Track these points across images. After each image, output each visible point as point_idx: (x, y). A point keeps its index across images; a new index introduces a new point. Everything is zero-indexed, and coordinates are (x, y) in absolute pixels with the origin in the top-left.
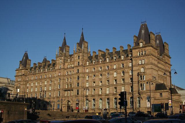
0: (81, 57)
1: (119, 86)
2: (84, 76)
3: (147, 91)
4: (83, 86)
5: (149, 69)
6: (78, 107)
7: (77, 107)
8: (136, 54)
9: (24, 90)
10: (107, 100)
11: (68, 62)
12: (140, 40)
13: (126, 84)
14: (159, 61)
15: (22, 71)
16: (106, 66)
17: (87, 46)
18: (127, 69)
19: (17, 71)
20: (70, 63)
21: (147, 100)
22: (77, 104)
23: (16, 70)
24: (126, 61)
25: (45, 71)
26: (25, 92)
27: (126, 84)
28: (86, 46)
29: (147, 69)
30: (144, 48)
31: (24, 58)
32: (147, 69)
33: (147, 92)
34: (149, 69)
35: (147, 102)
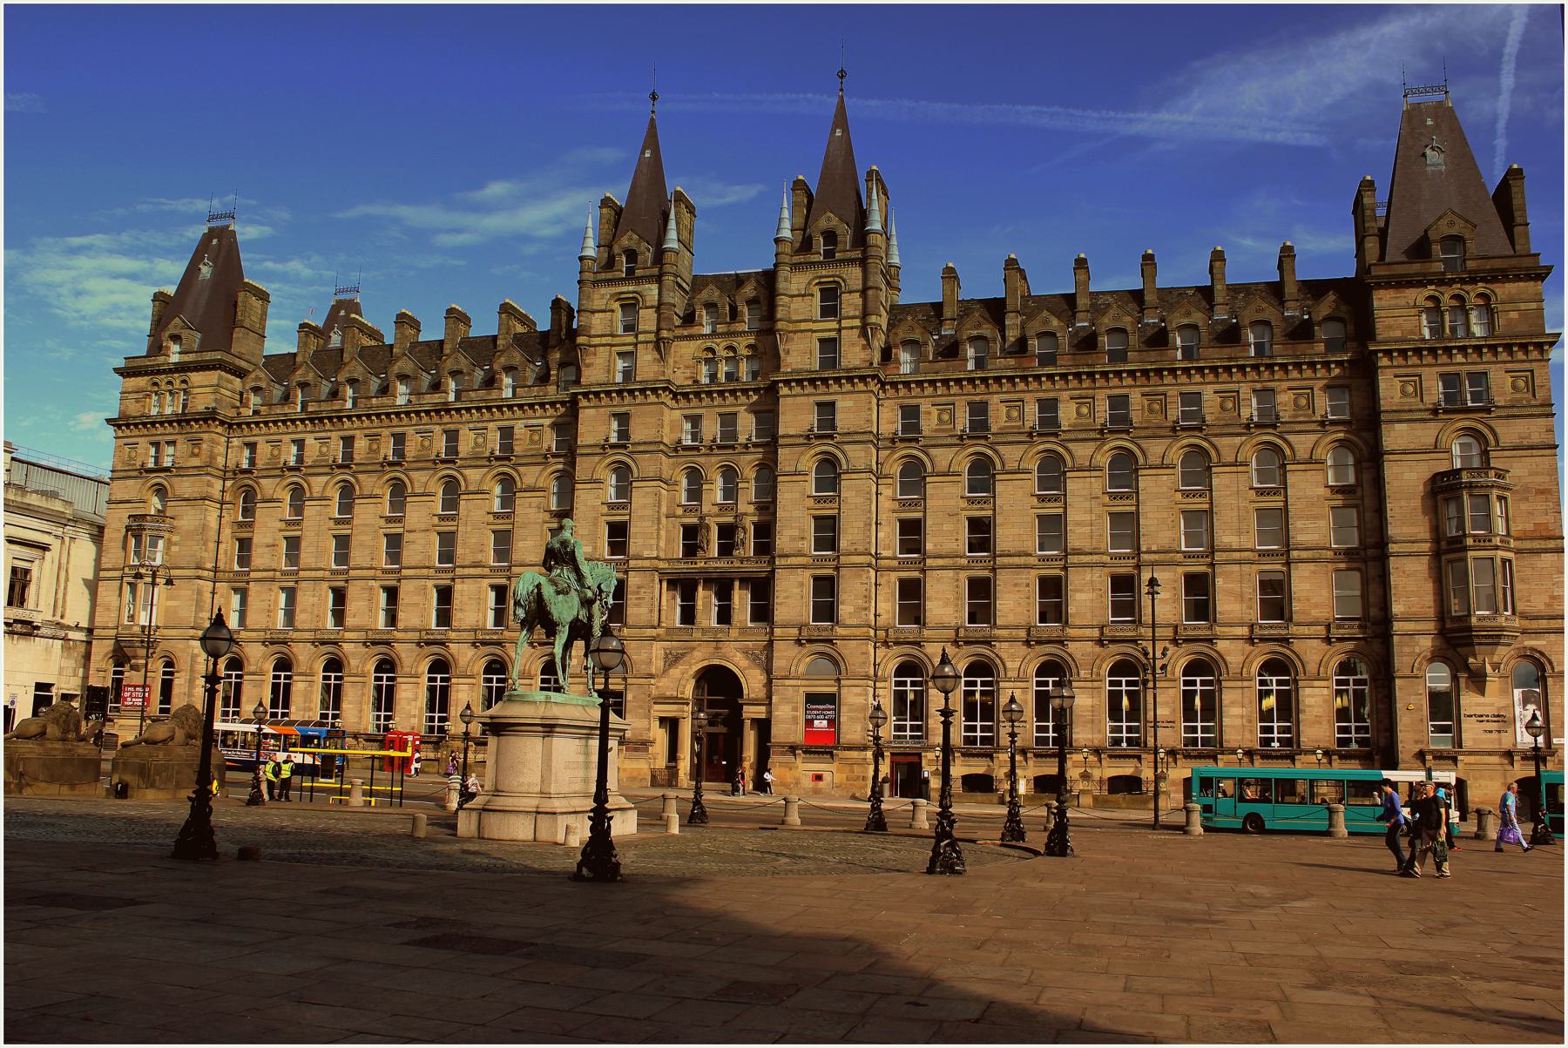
0: (851, 303)
1: (1236, 568)
6: (809, 723)
7: (820, 724)
8: (1409, 324)
9: (212, 546)
11: (695, 330)
13: (1304, 554)
15: (196, 378)
21: (1517, 693)
22: (812, 699)
23: (119, 371)
25: (437, 398)
26: (216, 570)
27: (1304, 554)
30: (1480, 287)
31: (206, 271)
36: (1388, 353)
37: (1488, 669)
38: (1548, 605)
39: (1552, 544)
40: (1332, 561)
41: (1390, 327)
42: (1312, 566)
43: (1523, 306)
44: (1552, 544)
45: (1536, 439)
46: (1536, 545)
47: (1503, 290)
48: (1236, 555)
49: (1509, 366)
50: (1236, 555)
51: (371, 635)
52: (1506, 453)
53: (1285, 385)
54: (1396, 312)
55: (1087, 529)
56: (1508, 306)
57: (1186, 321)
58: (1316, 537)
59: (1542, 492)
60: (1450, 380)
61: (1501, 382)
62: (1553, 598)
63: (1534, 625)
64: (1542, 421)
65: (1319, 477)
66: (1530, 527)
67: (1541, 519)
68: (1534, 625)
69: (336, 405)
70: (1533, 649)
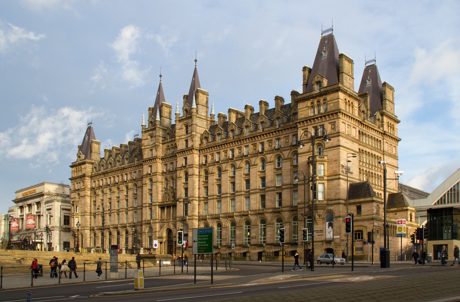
1: (270, 192)
2: (199, 172)
3: (329, 202)
4: (197, 196)
5: (333, 147)
8: (305, 113)
10: (244, 226)
12: (316, 77)
13: (285, 187)
14: (364, 130)
16: (243, 146)
17: (207, 102)
18: (288, 151)
19: (74, 169)
20: (170, 144)
21: (327, 223)
24: (284, 132)
27: (285, 187)
28: (204, 102)
29: (329, 148)
32: (329, 148)
33: (328, 205)
34: (333, 147)
35: (327, 228)
36: (299, 123)
37: (317, 217)
38: (335, 196)
39: (337, 177)
40: (291, 188)
41: (301, 114)
42: (287, 190)
43: (334, 101)
44: (337, 177)
45: (335, 144)
46: (333, 178)
47: (329, 97)
48: (270, 189)
49: (330, 121)
50: (270, 189)
51: (123, 225)
52: (327, 150)
53: (283, 136)
54: (303, 110)
55: (239, 185)
56: (330, 102)
57: (261, 121)
58: (288, 181)
59: (335, 161)
60: (316, 129)
61: (328, 128)
62: (336, 193)
63: (331, 202)
64: (337, 138)
65: (273, 166)
66: (332, 172)
67: (335, 169)
68: (331, 202)
69: (108, 170)
70: (330, 210)
